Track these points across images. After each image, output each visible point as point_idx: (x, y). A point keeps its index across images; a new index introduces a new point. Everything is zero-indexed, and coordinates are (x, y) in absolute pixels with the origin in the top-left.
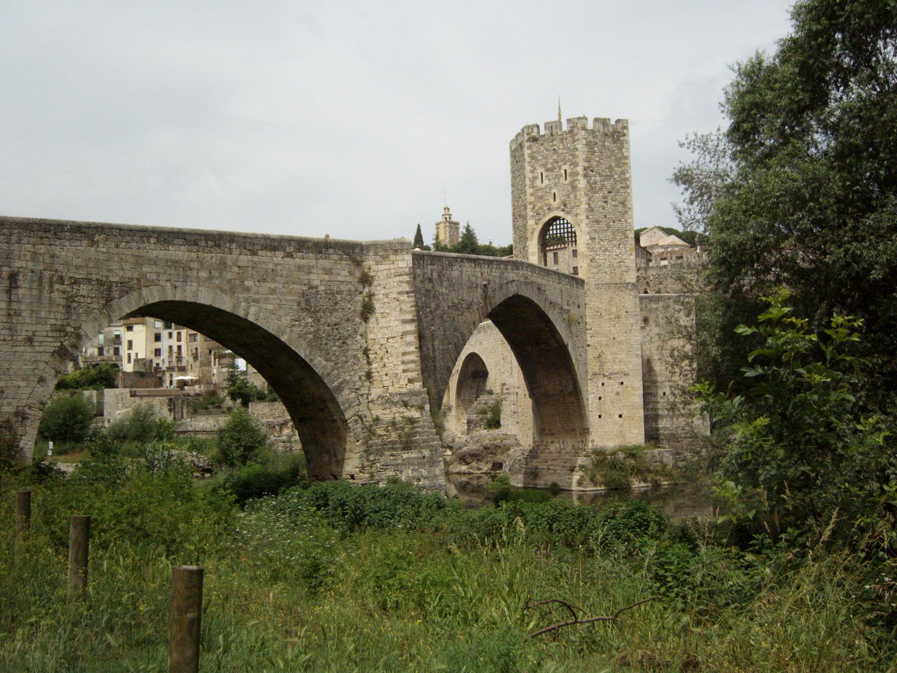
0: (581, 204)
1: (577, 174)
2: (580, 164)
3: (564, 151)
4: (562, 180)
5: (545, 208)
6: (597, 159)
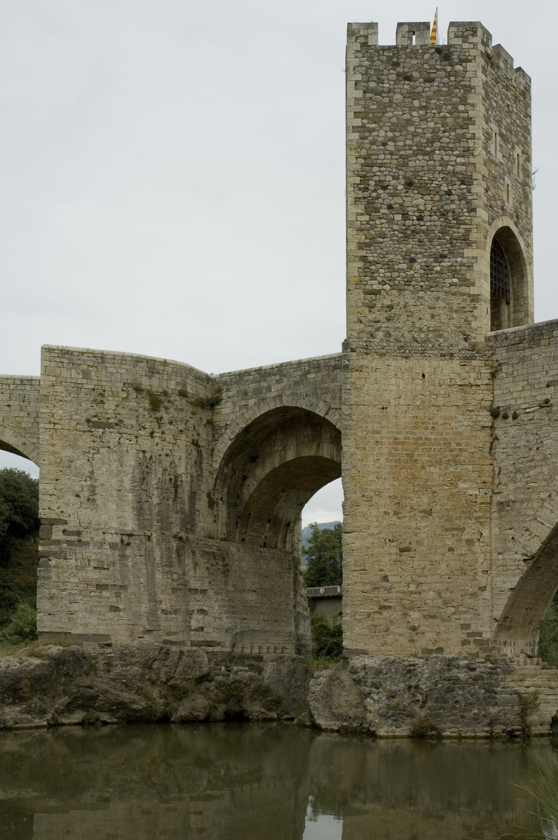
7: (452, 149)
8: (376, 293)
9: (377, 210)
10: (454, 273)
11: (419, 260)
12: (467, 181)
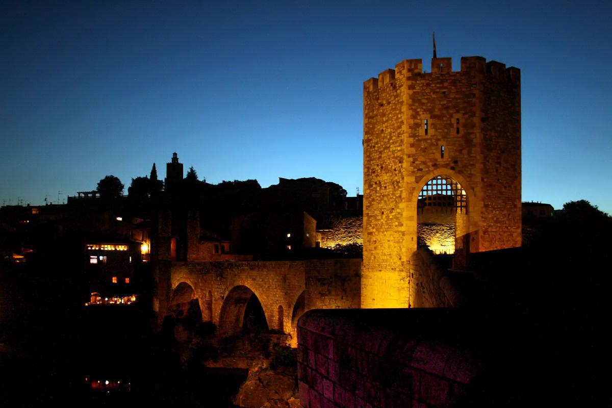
1: (473, 126)
2: (478, 114)
4: (453, 132)
5: (430, 164)
7: (396, 142)
9: (372, 186)
10: (397, 218)
11: (385, 213)
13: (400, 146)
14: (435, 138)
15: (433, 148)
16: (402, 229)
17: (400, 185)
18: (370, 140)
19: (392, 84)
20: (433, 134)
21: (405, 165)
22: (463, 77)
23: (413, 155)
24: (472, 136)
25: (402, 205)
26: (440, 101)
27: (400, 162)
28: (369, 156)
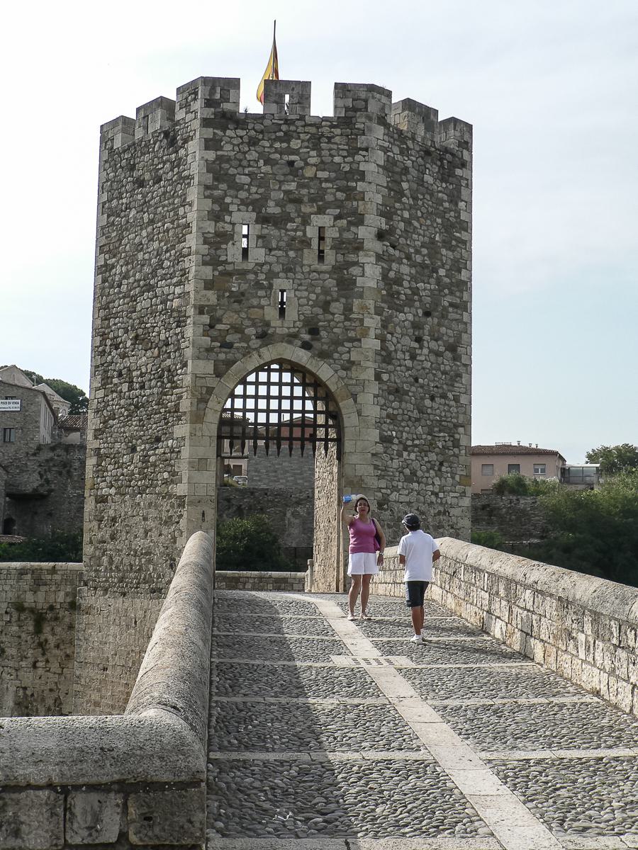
0: (365, 333)
1: (358, 246)
3: (321, 174)
4: (310, 257)
5: (251, 331)
6: (406, 214)
8: (102, 500)
12: (180, 323)
13: (179, 283)
14: (266, 268)
15: (261, 293)
16: (181, 489)
17: (175, 379)
18: (113, 266)
19: (166, 134)
20: (262, 260)
21: (189, 332)
22: (338, 131)
23: (212, 309)
24: (355, 271)
25: (182, 430)
26: (281, 182)
27: (178, 326)
28: (106, 307)
